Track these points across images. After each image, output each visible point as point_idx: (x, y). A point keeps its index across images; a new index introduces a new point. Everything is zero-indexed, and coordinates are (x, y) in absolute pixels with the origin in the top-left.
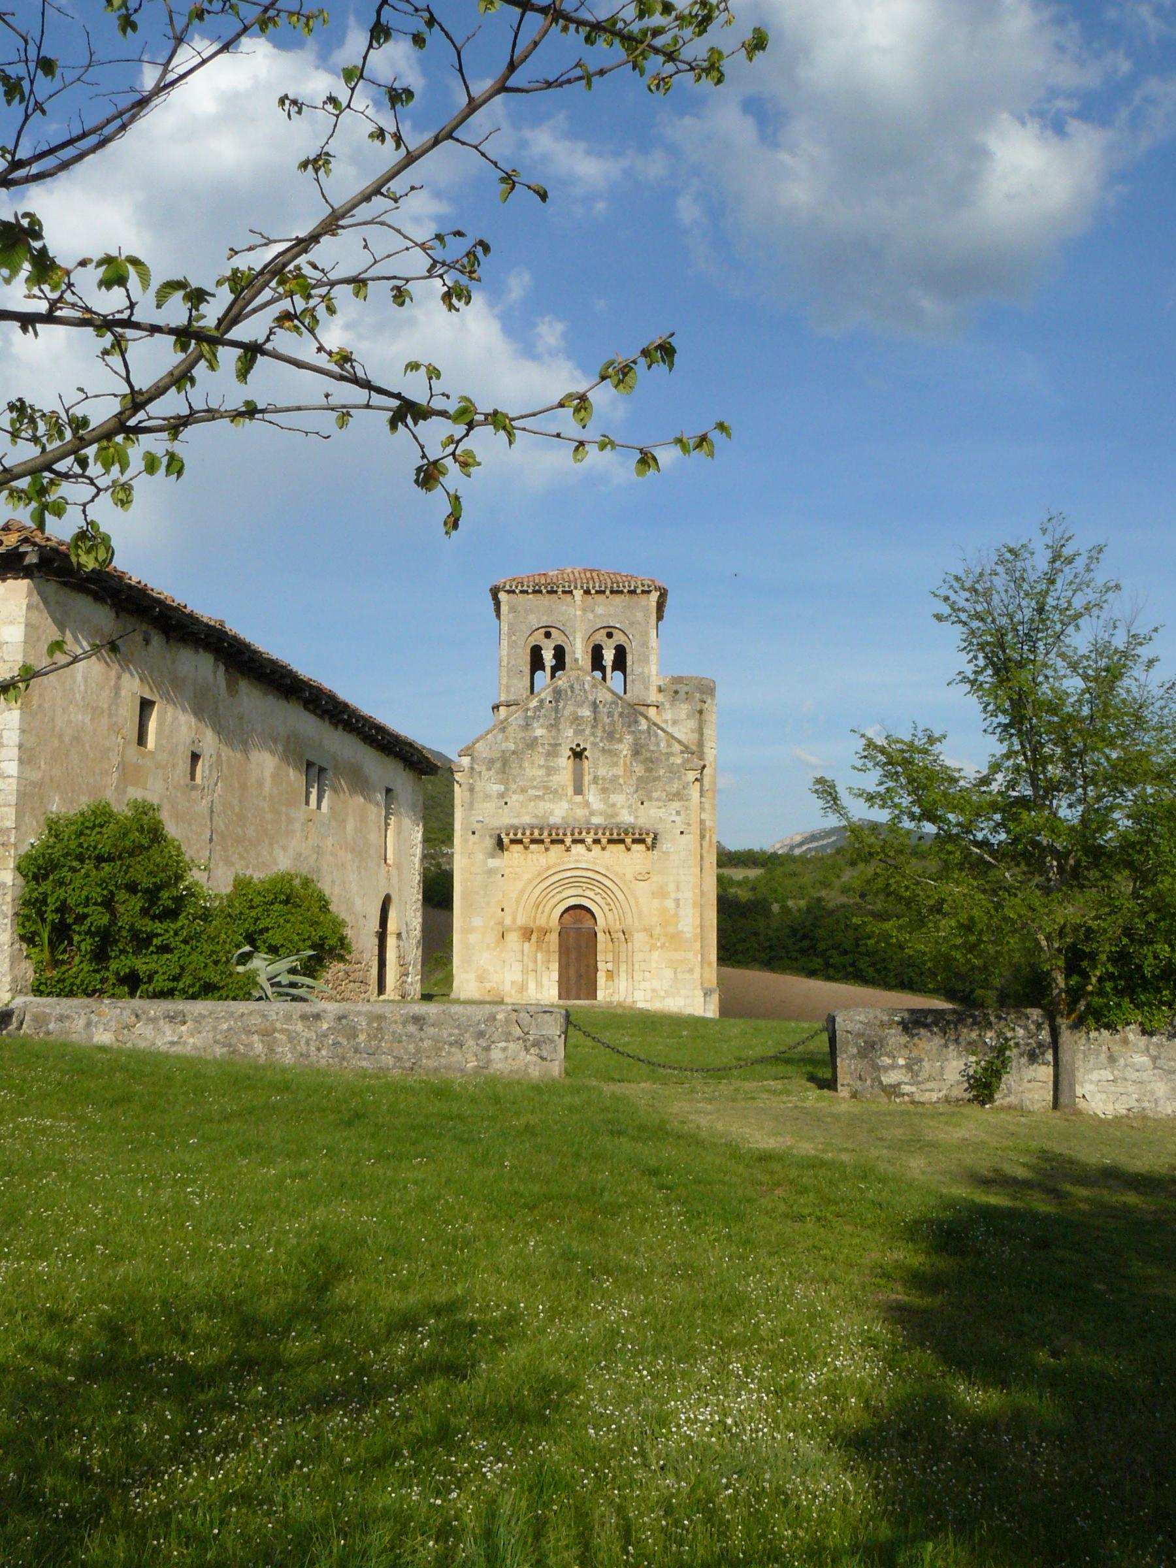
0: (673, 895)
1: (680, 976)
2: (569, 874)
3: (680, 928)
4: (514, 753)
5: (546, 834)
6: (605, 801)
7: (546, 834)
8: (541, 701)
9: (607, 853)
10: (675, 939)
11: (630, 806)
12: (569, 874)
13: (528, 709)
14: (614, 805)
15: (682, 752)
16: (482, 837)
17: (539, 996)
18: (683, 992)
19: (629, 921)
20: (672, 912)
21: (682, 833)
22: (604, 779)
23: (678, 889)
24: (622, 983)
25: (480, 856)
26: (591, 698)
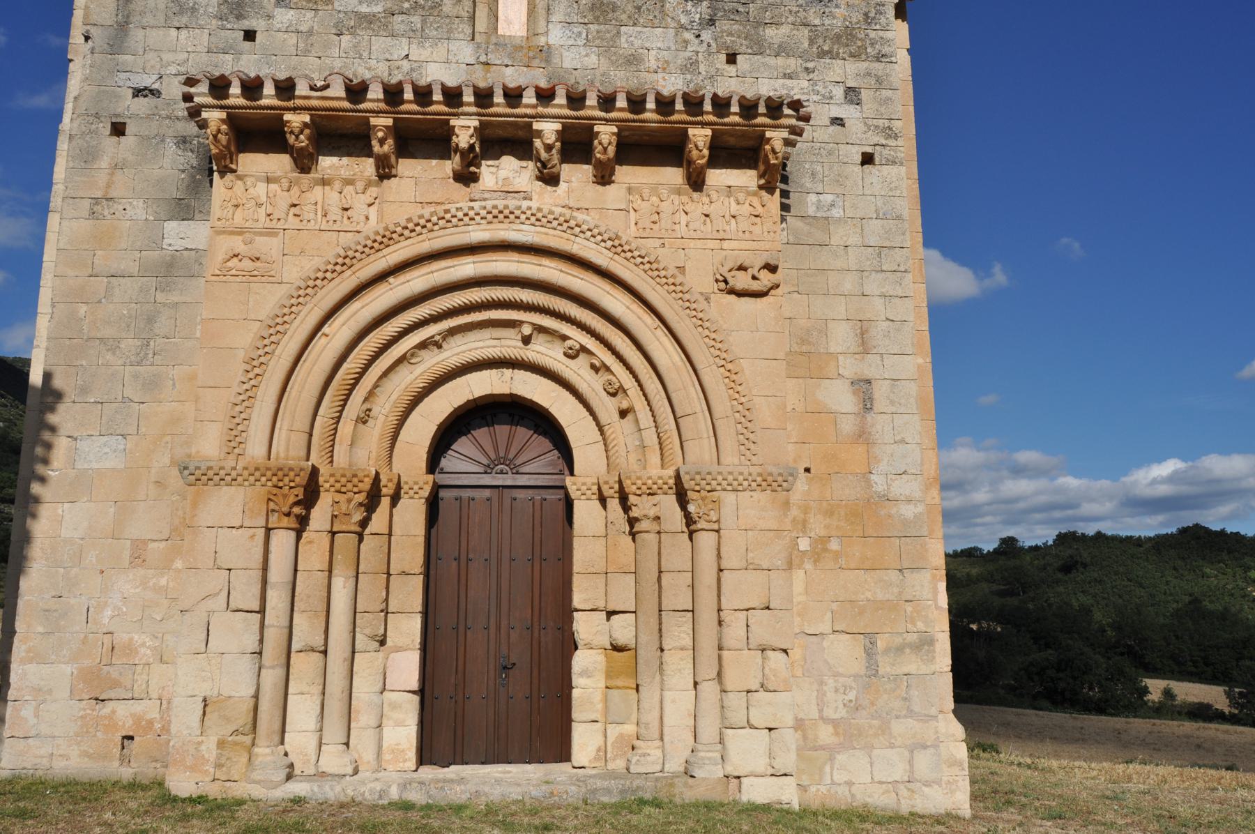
0: (849, 366)
1: (885, 668)
2: (467, 267)
3: (879, 482)
5: (375, 92)
6: (608, 47)
7: (375, 92)
9: (613, 194)
10: (866, 516)
11: (691, 66)
12: (467, 267)
14: (633, 60)
16: (152, 142)
17: (334, 760)
18: (898, 727)
19: (700, 451)
20: (848, 426)
21: (867, 159)
23: (865, 347)
24: (675, 697)
25: (139, 210)
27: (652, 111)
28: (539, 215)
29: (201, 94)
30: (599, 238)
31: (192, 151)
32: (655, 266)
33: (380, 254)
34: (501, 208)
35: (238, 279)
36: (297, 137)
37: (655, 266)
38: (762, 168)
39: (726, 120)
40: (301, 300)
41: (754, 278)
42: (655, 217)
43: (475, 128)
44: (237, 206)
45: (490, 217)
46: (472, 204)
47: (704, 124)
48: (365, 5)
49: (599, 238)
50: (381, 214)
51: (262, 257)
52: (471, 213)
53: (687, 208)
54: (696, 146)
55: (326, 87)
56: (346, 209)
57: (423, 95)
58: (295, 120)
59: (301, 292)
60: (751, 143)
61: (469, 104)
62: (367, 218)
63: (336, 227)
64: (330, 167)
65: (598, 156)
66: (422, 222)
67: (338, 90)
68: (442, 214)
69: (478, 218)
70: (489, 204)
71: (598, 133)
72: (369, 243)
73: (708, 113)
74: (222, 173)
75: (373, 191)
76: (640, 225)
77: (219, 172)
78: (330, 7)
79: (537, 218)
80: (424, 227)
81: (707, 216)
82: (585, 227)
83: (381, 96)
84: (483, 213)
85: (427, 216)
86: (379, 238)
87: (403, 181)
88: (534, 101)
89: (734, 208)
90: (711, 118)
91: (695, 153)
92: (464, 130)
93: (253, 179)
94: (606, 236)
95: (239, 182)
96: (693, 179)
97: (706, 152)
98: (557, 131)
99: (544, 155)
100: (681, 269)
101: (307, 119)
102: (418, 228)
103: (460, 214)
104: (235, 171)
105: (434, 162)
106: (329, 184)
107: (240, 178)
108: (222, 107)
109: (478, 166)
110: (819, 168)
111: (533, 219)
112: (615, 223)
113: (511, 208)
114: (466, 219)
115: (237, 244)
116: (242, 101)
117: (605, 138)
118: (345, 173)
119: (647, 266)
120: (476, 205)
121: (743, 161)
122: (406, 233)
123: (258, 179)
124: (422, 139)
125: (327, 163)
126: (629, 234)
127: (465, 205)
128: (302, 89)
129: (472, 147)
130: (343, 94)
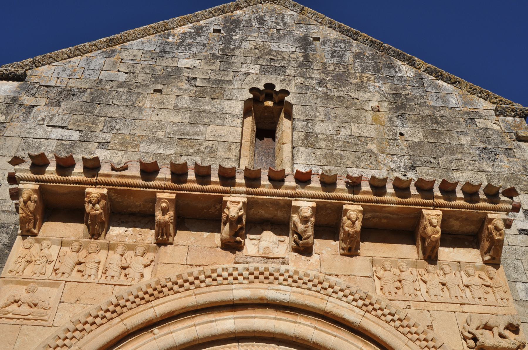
4: (122, 84)
5: (165, 173)
8: (199, 31)
9: (359, 264)
13: (169, 35)
15: (499, 112)
22: (328, 139)
26: (298, 32)
27: (392, 195)
28: (296, 277)
29: (23, 170)
30: (351, 298)
31: (7, 233)
32: (405, 323)
33: (149, 305)
34: (262, 269)
35: (12, 322)
36: (94, 205)
37: (405, 323)
38: (486, 244)
39: (453, 203)
40: (67, 342)
41: (501, 336)
42: (398, 284)
43: (244, 203)
44: (29, 262)
45: (251, 277)
46: (236, 266)
47: (436, 206)
48: (161, 150)
49: (351, 298)
50: (154, 273)
51: (41, 304)
52: (235, 274)
53: (425, 278)
54: (431, 224)
55: (125, 168)
56: (124, 268)
57: (203, 175)
58: (94, 192)
59: (69, 335)
60: (471, 228)
61: (240, 185)
62: (142, 276)
63: (112, 282)
64: (116, 236)
65: (347, 229)
66: (191, 279)
67: (135, 171)
68: (209, 273)
69: (240, 278)
70: (252, 267)
71: (347, 210)
72: (141, 294)
73: (438, 197)
74: (24, 236)
75: (150, 256)
76: (386, 289)
77: (22, 235)
78: (137, 150)
79: (294, 280)
80: (192, 283)
81: (444, 284)
82: (337, 288)
83: (169, 176)
84: (246, 274)
85: (196, 274)
86: (150, 291)
87: (177, 248)
88: (294, 184)
89: (466, 280)
90: (442, 201)
91: (429, 229)
92: (234, 205)
93: (49, 242)
94: (357, 296)
95: (37, 245)
96: (428, 254)
97: (438, 228)
98: (312, 208)
99: (301, 227)
100: (430, 327)
101: (105, 191)
102: (187, 285)
103: (225, 274)
104: (35, 235)
105: (206, 234)
106: (113, 249)
107: (38, 241)
108: (37, 181)
109: (244, 238)
110: (519, 263)
111: (290, 281)
112: (366, 287)
113: (271, 270)
114: (230, 278)
115: (21, 292)
116: (55, 176)
117: (353, 215)
118: (127, 241)
119: (398, 323)
120: (240, 267)
121: (466, 243)
122: (176, 287)
123: (54, 243)
124: (199, 214)
125: (116, 232)
126: (377, 295)
127: (230, 266)
128: (105, 169)
129: (240, 218)
130: (139, 174)
